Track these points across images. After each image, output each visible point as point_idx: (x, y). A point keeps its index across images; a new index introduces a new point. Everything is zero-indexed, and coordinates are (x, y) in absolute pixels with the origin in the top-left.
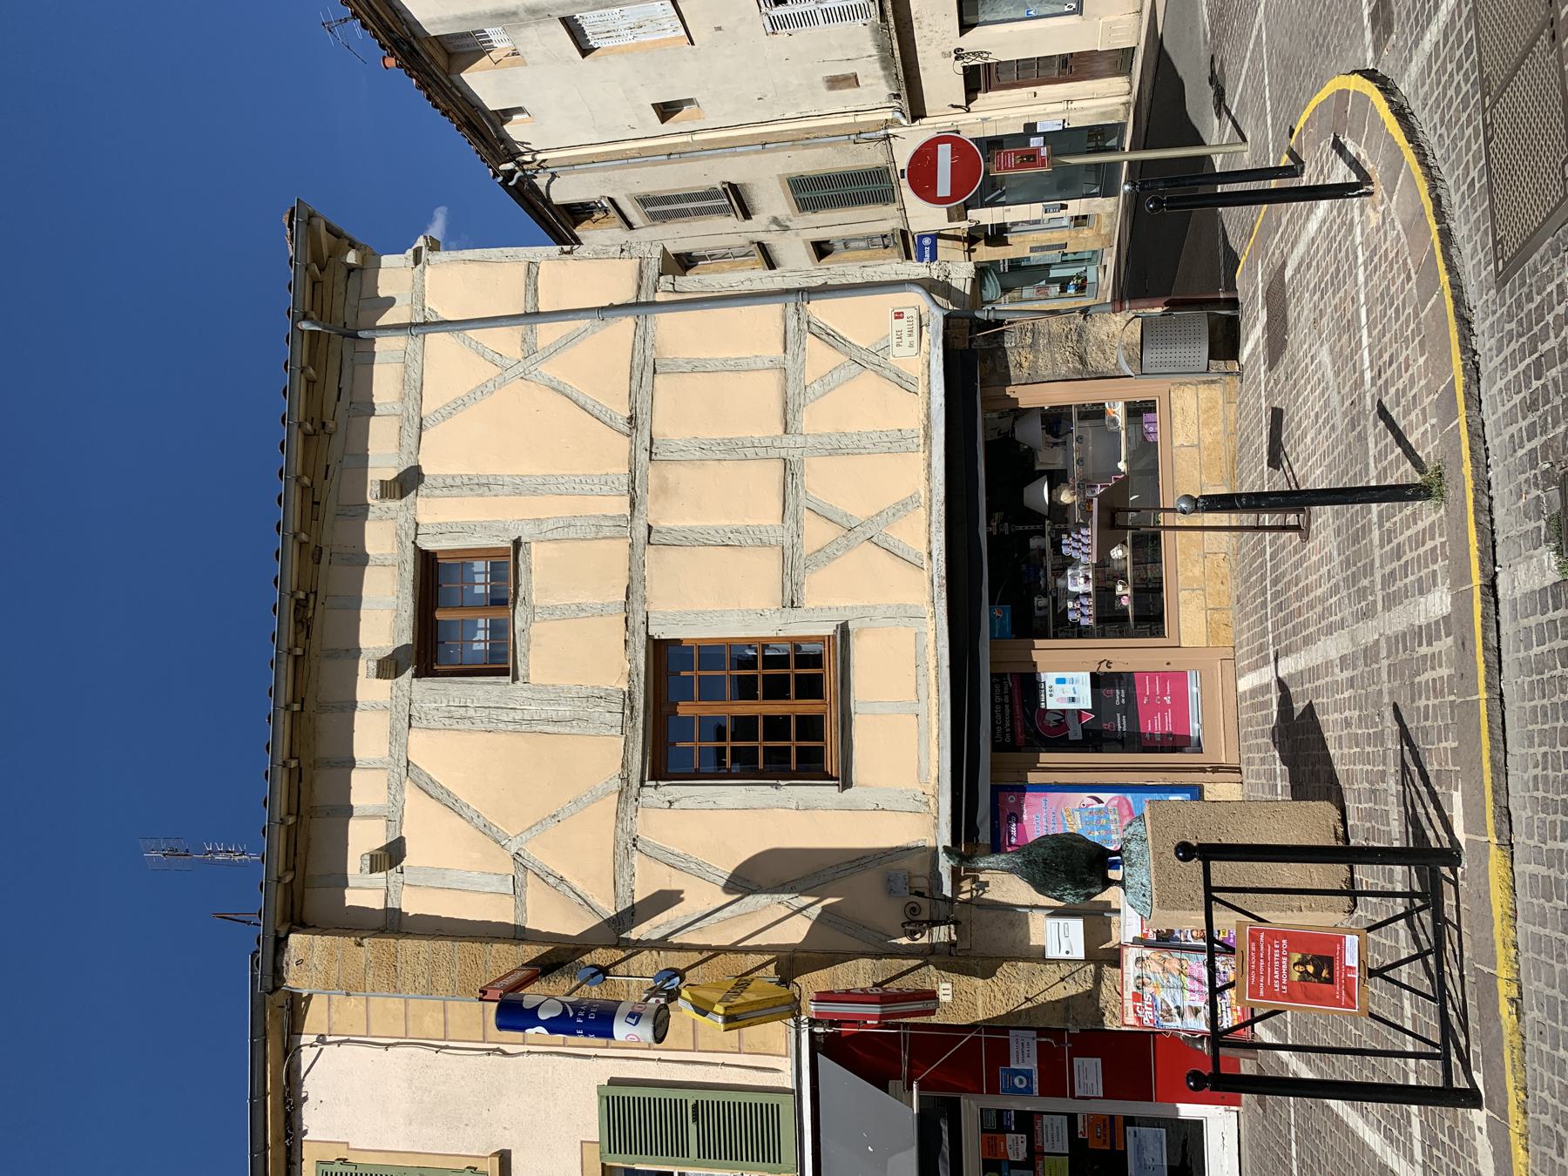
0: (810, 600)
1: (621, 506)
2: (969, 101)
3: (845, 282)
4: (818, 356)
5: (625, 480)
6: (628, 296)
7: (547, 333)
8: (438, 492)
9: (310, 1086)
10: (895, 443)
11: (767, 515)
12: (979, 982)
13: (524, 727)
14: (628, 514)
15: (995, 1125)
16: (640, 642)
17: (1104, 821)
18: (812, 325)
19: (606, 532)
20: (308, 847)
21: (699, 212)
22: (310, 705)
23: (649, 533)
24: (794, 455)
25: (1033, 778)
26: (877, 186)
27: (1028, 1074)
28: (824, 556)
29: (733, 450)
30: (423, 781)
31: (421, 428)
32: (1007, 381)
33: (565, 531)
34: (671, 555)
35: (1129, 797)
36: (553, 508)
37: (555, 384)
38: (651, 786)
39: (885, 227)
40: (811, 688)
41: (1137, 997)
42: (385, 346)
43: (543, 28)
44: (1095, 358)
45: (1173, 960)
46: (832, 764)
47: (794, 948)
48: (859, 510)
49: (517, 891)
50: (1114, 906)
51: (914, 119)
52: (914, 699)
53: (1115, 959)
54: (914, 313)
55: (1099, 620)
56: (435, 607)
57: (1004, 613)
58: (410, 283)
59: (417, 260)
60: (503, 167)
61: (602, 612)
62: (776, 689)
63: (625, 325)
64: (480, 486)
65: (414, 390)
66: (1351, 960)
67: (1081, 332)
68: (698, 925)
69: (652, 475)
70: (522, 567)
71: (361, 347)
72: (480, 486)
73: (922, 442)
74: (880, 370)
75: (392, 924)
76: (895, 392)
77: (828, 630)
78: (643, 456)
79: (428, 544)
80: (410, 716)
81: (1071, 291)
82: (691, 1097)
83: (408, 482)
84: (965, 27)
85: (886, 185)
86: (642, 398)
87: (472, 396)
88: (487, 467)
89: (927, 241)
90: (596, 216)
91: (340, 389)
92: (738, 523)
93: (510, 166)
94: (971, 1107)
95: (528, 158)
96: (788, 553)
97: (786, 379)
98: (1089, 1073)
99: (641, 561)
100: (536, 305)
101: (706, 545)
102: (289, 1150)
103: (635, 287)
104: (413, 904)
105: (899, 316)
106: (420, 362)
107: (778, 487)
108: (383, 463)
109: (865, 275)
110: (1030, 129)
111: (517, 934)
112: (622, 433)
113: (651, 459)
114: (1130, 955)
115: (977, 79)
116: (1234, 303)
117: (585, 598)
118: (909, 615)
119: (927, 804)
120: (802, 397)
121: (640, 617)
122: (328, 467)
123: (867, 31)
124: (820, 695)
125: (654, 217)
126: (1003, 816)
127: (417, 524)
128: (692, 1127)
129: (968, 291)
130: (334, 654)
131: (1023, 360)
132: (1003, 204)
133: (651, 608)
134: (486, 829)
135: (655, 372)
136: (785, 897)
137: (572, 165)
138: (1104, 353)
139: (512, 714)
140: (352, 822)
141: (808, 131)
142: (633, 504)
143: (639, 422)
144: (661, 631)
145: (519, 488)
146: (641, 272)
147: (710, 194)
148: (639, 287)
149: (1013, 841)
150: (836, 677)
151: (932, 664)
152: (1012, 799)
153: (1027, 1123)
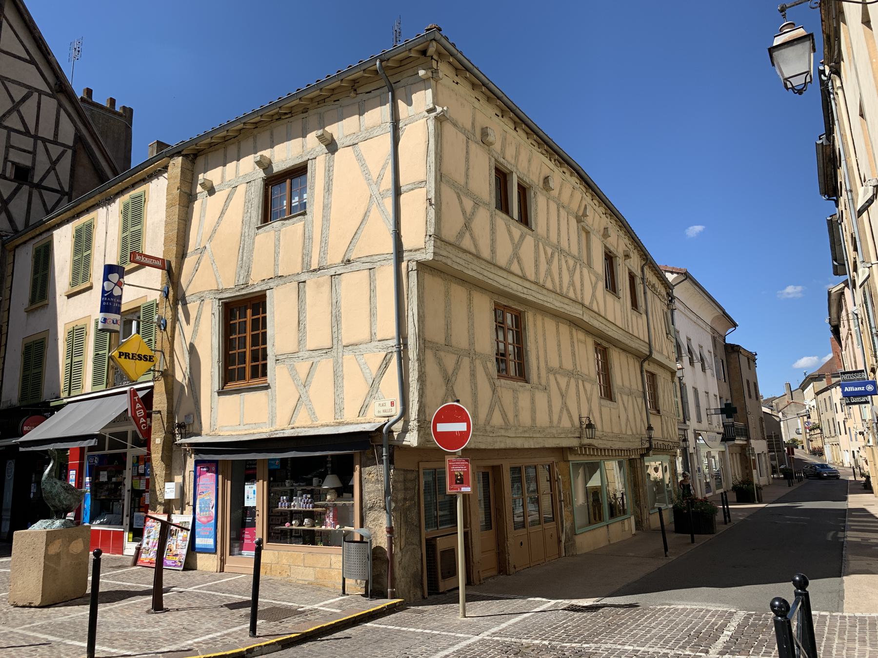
1: (314, 266)
3: (410, 371)
4: (375, 359)
6: (406, 244)
8: (327, 164)
10: (338, 408)
11: (311, 344)
14: (311, 269)
17: (206, 509)
18: (391, 354)
19: (305, 259)
20: (215, 150)
22: (255, 131)
23: (303, 282)
25: (220, 477)
31: (353, 145)
35: (213, 521)
37: (368, 214)
38: (219, 303)
46: (231, 386)
47: (173, 376)
48: (312, 390)
50: (184, 512)
52: (245, 423)
54: (393, 413)
58: (418, 112)
63: (390, 248)
68: (182, 334)
70: (295, 219)
73: (338, 421)
80: (250, 182)
87: (366, 168)
91: (370, 92)
96: (296, 355)
97: (367, 343)
99: (292, 280)
100: (405, 192)
101: (299, 312)
103: (410, 248)
105: (392, 404)
106: (382, 133)
108: (337, 130)
109: (413, 382)
112: (344, 257)
113: (331, 276)
117: (281, 255)
119: (213, 431)
120: (359, 353)
121: (272, 285)
122: (338, 100)
126: (208, 465)
127: (315, 158)
129: (404, 443)
131: (372, 475)
135: (370, 269)
136: (188, 370)
138: (374, 520)
142: (315, 270)
143: (348, 266)
145: (326, 207)
146: (418, 250)
148: (411, 251)
149: (202, 469)
150: (259, 384)
151: (255, 431)
152: (214, 469)
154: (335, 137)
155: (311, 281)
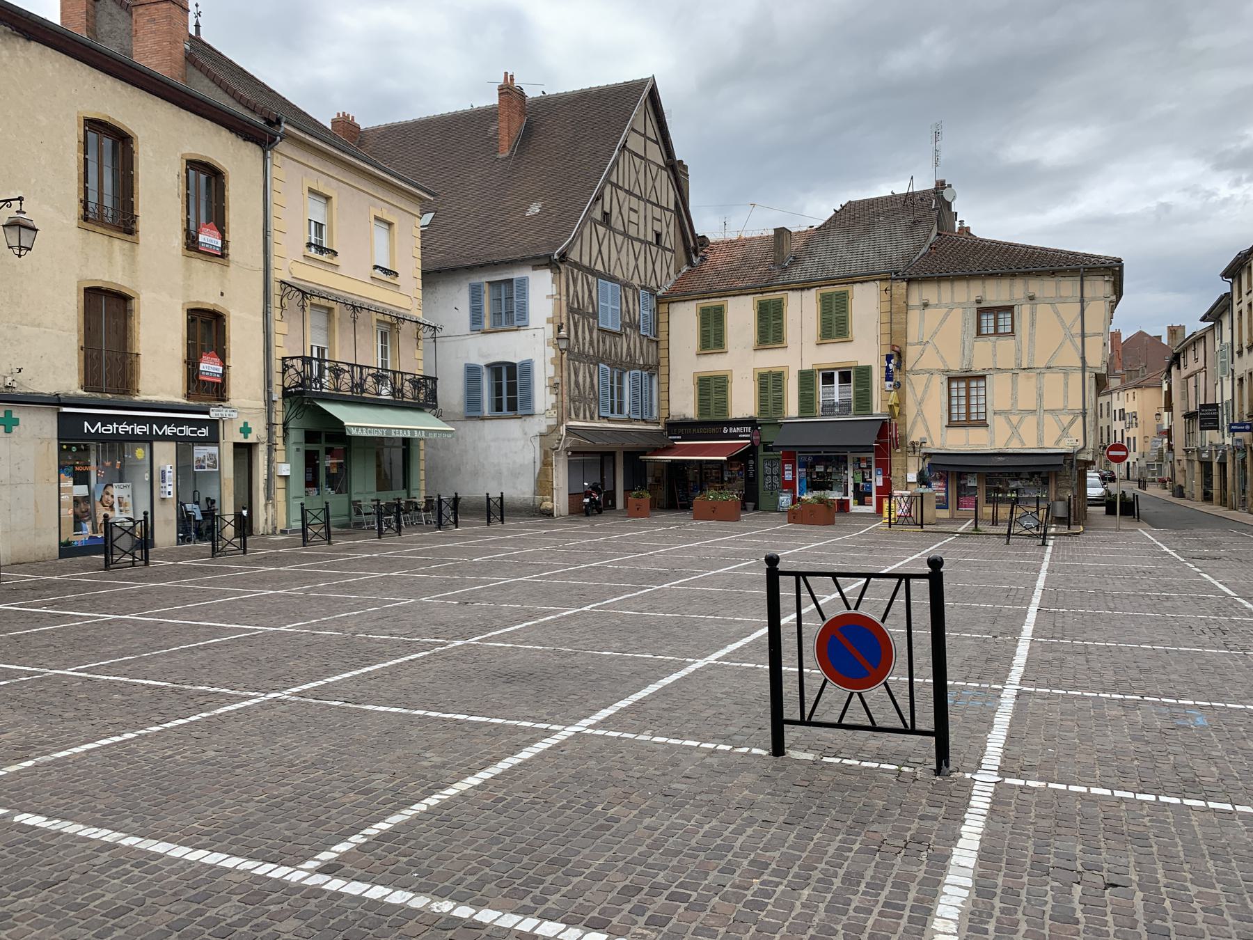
4: (1066, 419)
7: (1078, 341)
10: (1040, 440)
11: (1021, 406)
15: (868, 461)
16: (985, 373)
49: (920, 343)
63: (1080, 365)
65: (1063, 300)
69: (1033, 374)
78: (1038, 371)
86: (1057, 370)
94: (872, 455)
105: (1077, 441)
133: (995, 376)
139: (965, 337)
142: (1024, 369)
155: (1022, 374)
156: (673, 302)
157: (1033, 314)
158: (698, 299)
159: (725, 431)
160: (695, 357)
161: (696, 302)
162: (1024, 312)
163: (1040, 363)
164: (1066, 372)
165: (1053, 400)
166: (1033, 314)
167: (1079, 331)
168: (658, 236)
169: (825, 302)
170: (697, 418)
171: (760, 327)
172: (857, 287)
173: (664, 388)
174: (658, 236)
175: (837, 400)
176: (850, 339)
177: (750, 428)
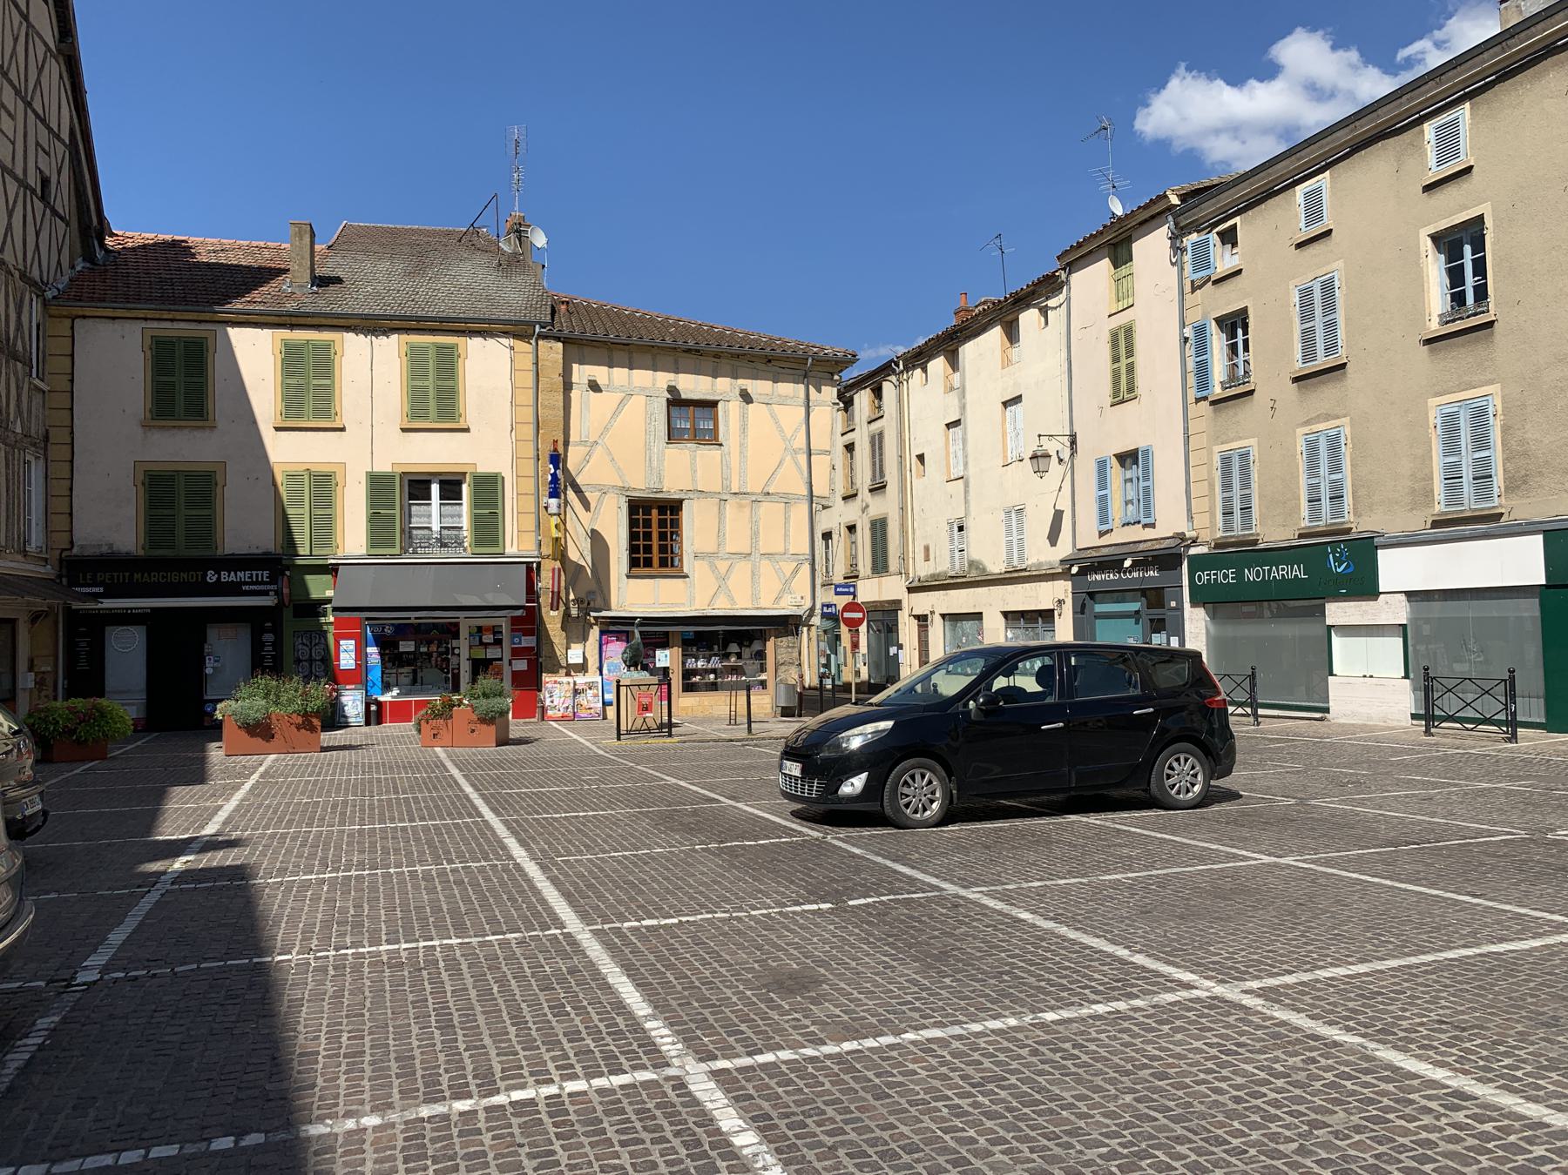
0: (697, 563)
2: (915, 616)
5: (745, 491)
6: (814, 494)
7: (803, 459)
9: (491, 342)
10: (755, 596)
11: (730, 547)
12: (559, 625)
13: (648, 447)
15: (496, 631)
21: (874, 464)
24: (752, 558)
26: (880, 565)
27: (520, 643)
28: (714, 568)
29: (755, 535)
30: (625, 401)
32: (776, 637)
33: (725, 464)
34: (716, 509)
36: (734, 460)
39: (860, 567)
40: (663, 563)
41: (555, 682)
42: (801, 387)
43: (957, 409)
44: (783, 668)
45: (570, 694)
49: (582, 443)
51: (908, 588)
53: (568, 674)
55: (687, 670)
56: (695, 406)
57: (691, 636)
59: (834, 404)
60: (901, 362)
61: (694, 480)
62: (663, 549)
63: (805, 492)
64: (744, 429)
66: (648, 715)
67: (792, 664)
69: (746, 501)
71: (801, 378)
72: (744, 429)
74: (783, 591)
75: (568, 386)
76: (775, 595)
77: (685, 570)
79: (720, 405)
81: (822, 670)
82: (499, 511)
83: (746, 397)
84: (943, 616)
85: (880, 569)
86: (776, 498)
88: (751, 431)
89: (852, 590)
90: (876, 401)
92: (727, 535)
93: (901, 367)
95: (905, 377)
98: (521, 665)
102: (464, 332)
104: (574, 394)
105: (802, 598)
107: (742, 551)
110: (900, 647)
111: (566, 443)
114: (570, 679)
115: (922, 619)
116: (800, 716)
117: (699, 473)
118: (692, 599)
123: (945, 569)
124: (661, 566)
125: (873, 438)
128: (487, 511)
130: (676, 362)
132: (868, 632)
134: (606, 429)
137: (900, 401)
140: (606, 368)
141: (907, 532)
142: (735, 494)
144: (685, 504)
147: (882, 474)
152: (624, 638)
153: (498, 642)
154: (749, 391)
155: (732, 501)
156: (84, 317)
157: (744, 417)
158: (146, 319)
159: (211, 577)
160: (140, 430)
161: (144, 324)
162: (730, 412)
163: (754, 486)
164: (787, 500)
165: (771, 541)
166: (744, 417)
167: (804, 446)
168: (45, 182)
169: (415, 359)
170: (141, 553)
171: (286, 387)
172: (475, 344)
173: (60, 488)
174: (45, 182)
175: (436, 527)
176: (462, 425)
177: (266, 573)
